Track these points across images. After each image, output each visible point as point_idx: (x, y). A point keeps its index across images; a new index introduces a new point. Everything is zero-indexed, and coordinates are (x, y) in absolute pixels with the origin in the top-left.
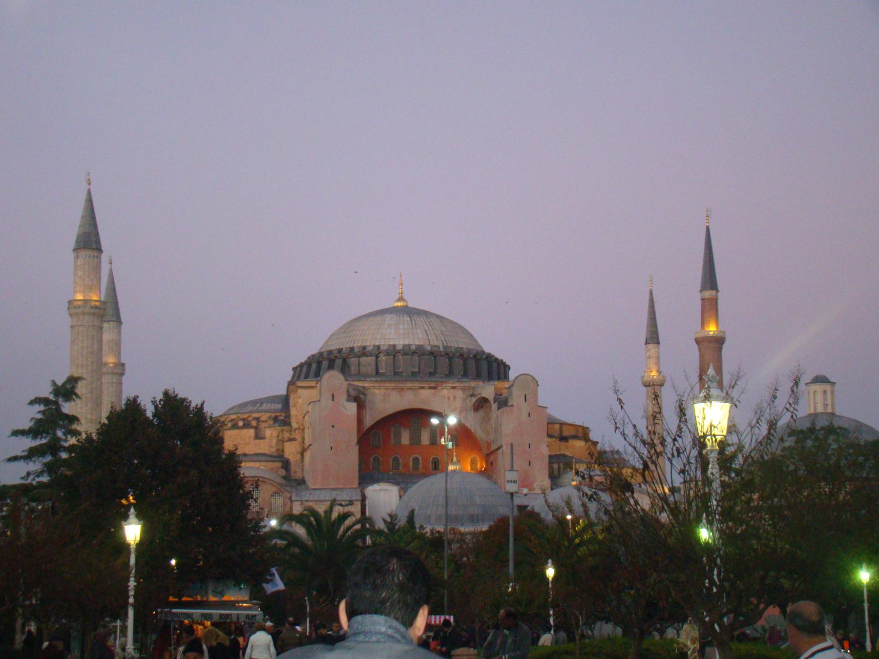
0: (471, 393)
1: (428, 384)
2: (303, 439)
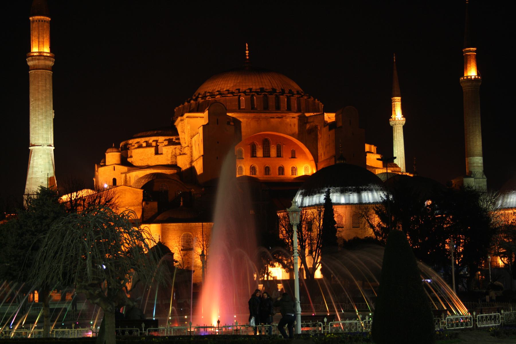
0: (306, 121)
1: (276, 115)
2: (191, 152)
